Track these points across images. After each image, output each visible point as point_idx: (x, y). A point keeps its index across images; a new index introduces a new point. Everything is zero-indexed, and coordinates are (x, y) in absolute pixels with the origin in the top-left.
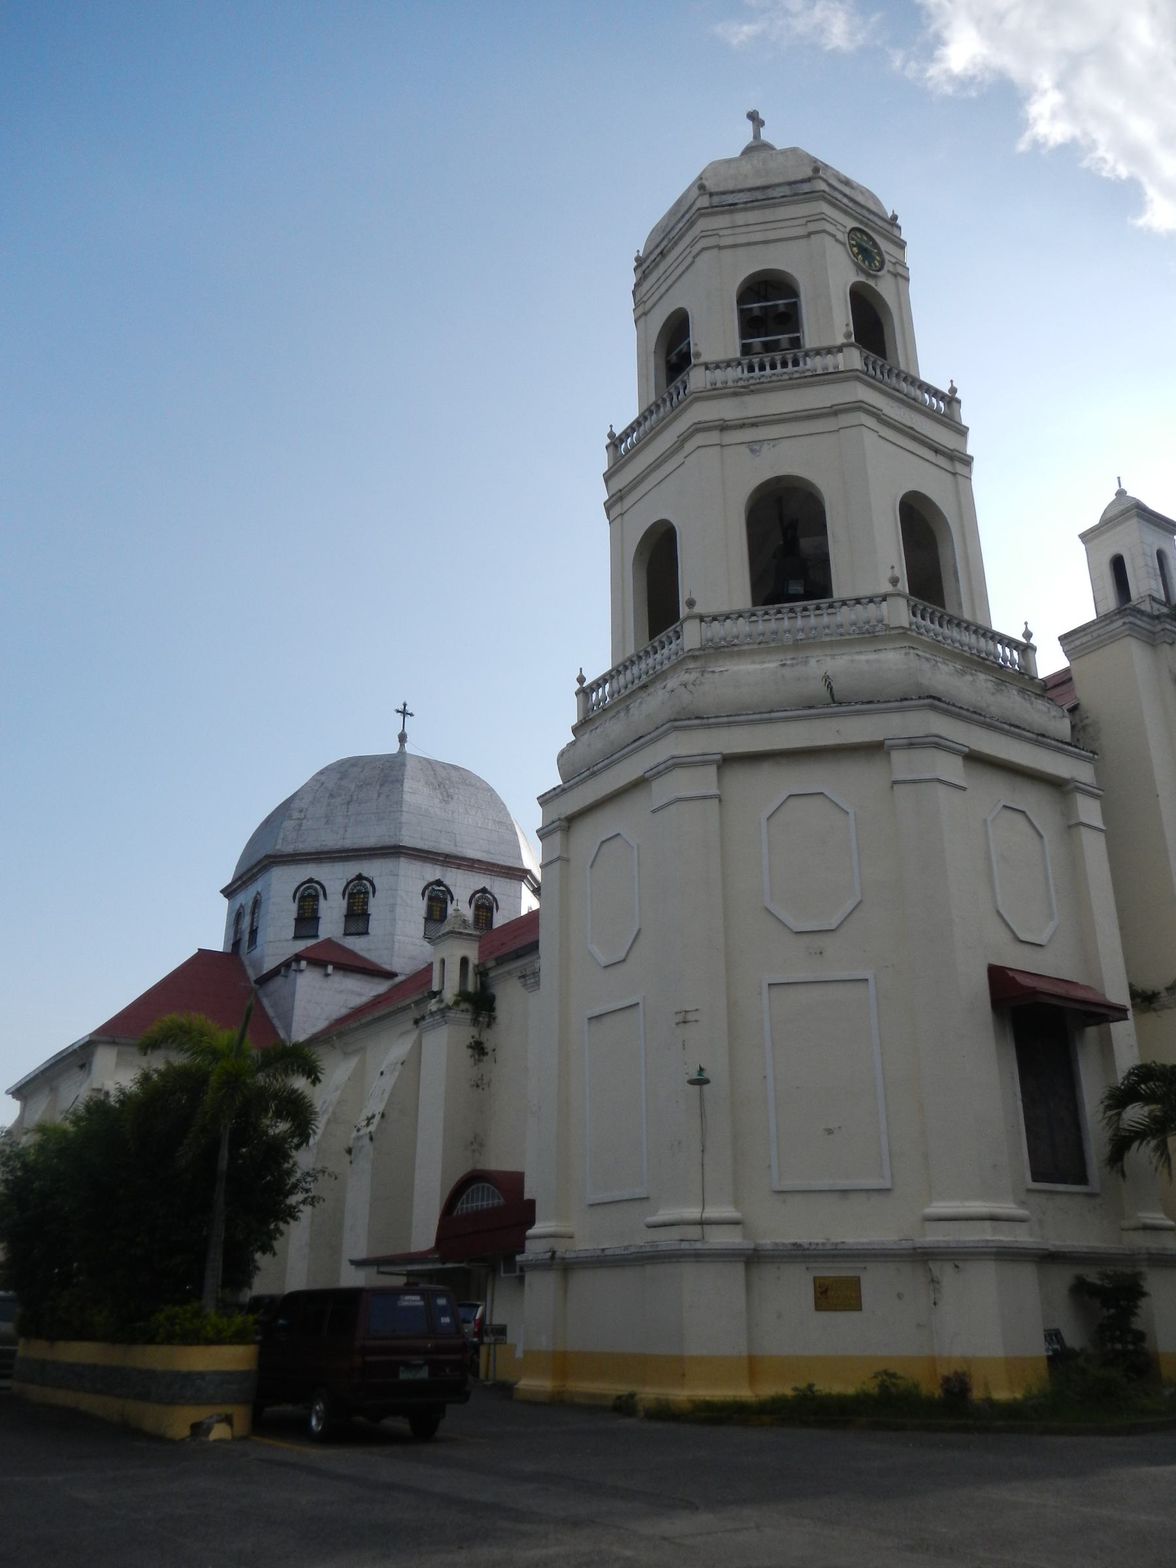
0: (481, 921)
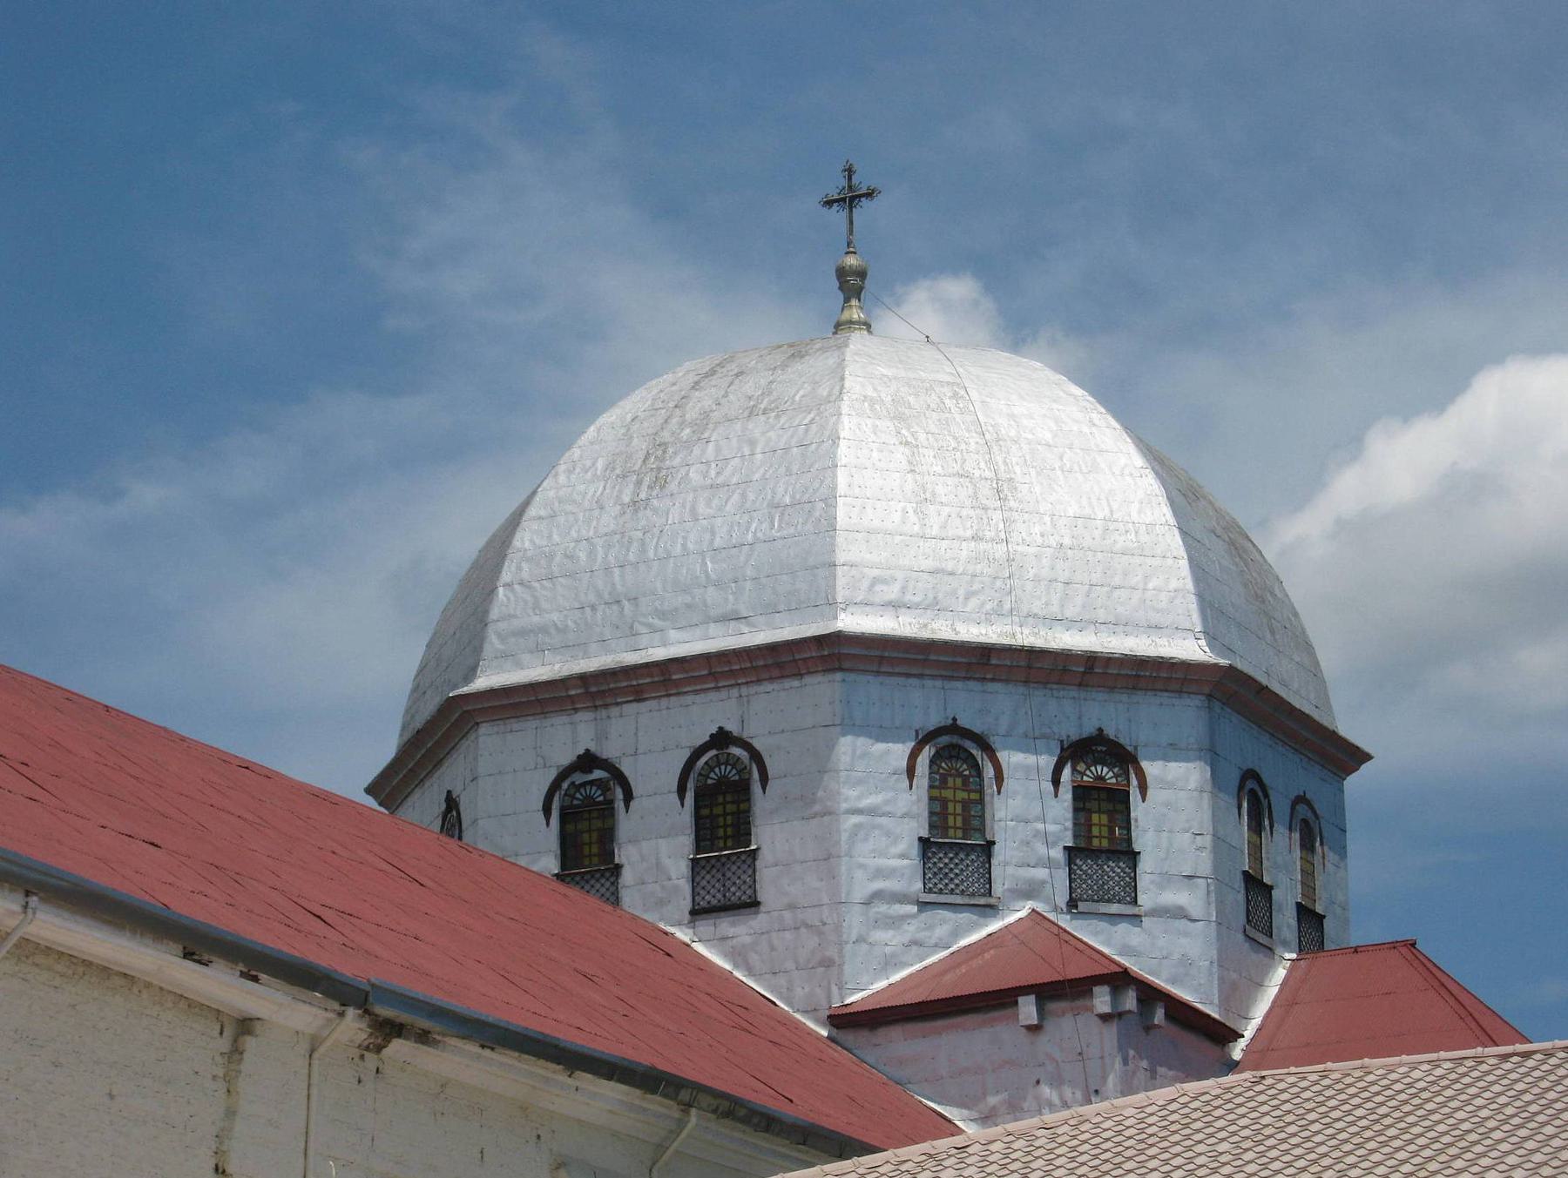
0: (721, 832)
